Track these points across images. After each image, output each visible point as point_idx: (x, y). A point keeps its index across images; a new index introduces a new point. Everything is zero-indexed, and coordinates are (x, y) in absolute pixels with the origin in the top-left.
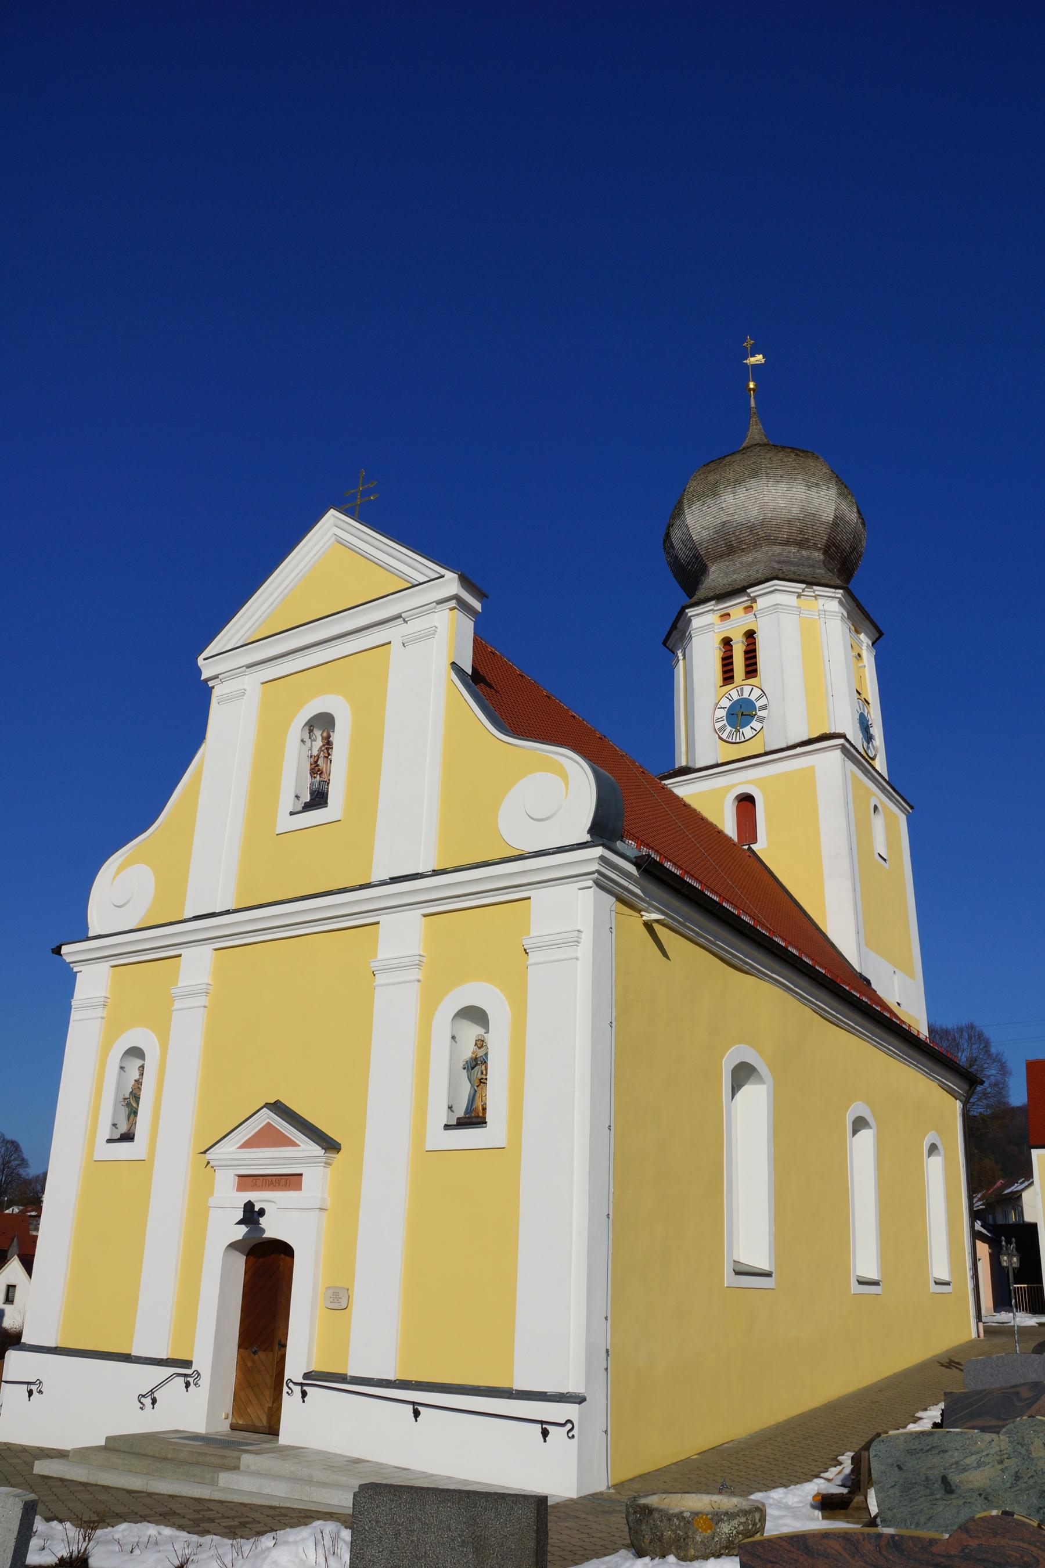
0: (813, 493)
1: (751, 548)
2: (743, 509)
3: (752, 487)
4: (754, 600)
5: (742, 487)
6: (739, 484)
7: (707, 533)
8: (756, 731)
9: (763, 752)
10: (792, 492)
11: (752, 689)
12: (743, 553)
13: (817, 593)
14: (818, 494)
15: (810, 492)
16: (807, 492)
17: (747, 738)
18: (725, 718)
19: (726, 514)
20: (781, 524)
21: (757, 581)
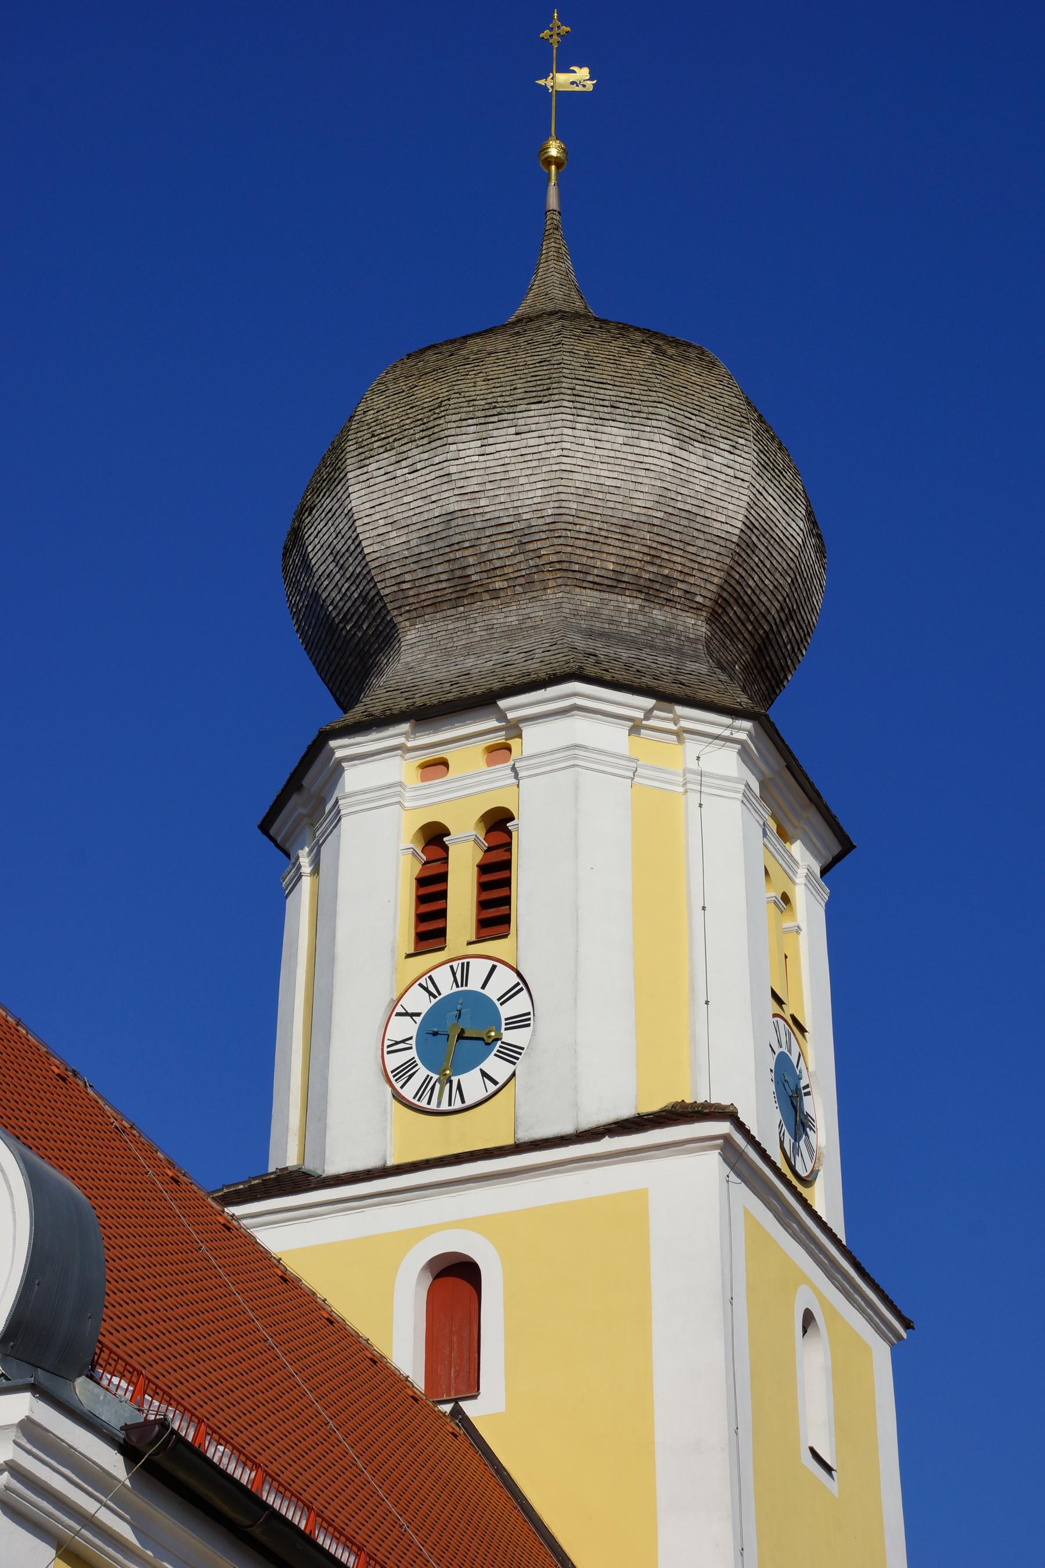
0: (693, 458)
1: (519, 589)
2: (504, 483)
3: (533, 427)
4: (514, 729)
5: (505, 424)
6: (499, 414)
7: (404, 539)
8: (495, 1083)
9: (510, 1141)
10: (637, 450)
11: (494, 967)
12: (494, 602)
13: (684, 724)
14: (704, 462)
15: (685, 455)
16: (678, 452)
17: (469, 1102)
18: (413, 1042)
19: (457, 492)
20: (603, 533)
21: (526, 679)
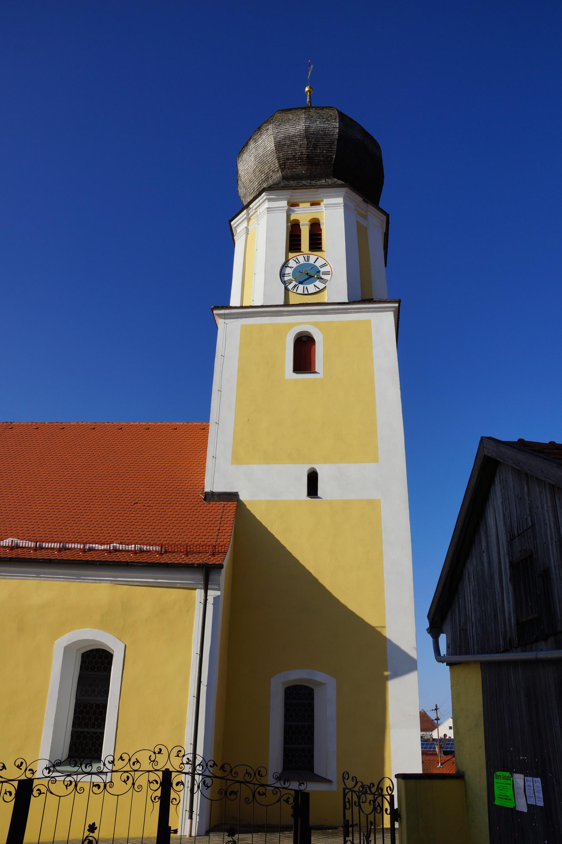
8: (319, 289)
11: (318, 258)
18: (291, 275)
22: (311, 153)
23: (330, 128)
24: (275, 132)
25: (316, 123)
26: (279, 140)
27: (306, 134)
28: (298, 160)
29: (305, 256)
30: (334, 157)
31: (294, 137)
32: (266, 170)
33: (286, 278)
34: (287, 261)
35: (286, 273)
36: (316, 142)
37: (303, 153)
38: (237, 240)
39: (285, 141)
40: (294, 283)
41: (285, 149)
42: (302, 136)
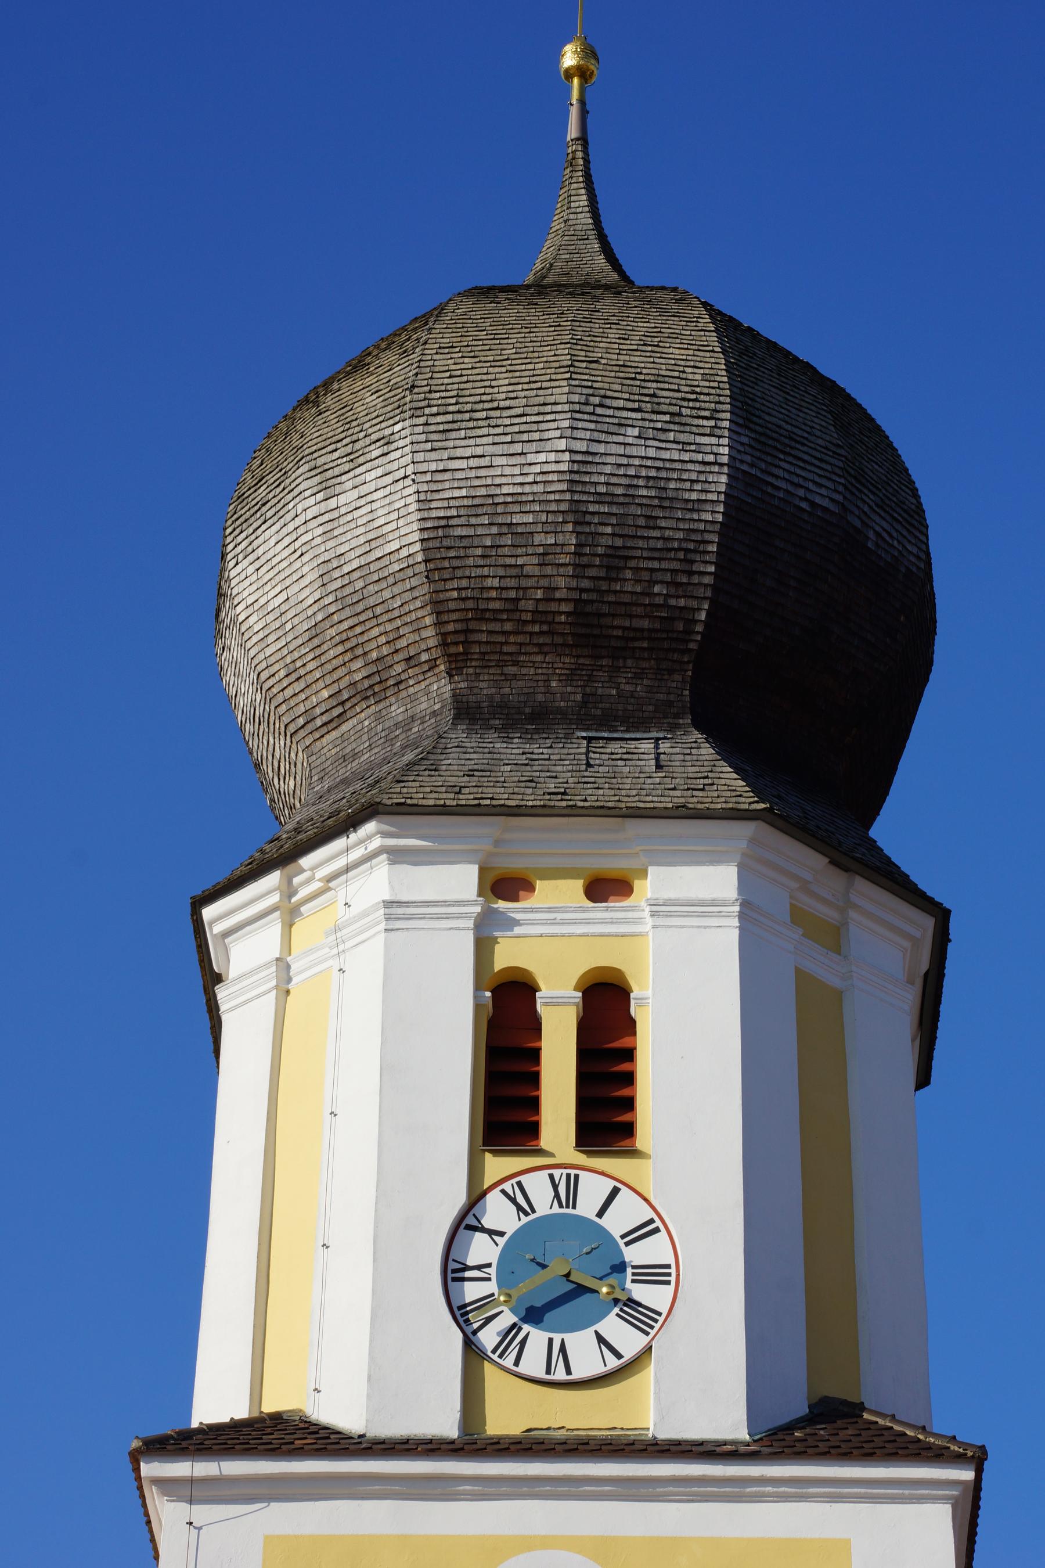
8: (619, 1356)
11: (615, 1191)
18: (492, 1271)
22: (594, 596)
23: (690, 466)
24: (423, 467)
25: (620, 439)
26: (441, 513)
27: (576, 497)
28: (533, 622)
29: (557, 1173)
30: (703, 616)
31: (516, 508)
32: (373, 645)
33: (472, 1291)
34: (476, 1198)
35: (470, 1262)
36: (619, 542)
37: (558, 595)
38: (232, 1009)
39: (473, 521)
40: (508, 1318)
41: (470, 561)
42: (554, 507)
